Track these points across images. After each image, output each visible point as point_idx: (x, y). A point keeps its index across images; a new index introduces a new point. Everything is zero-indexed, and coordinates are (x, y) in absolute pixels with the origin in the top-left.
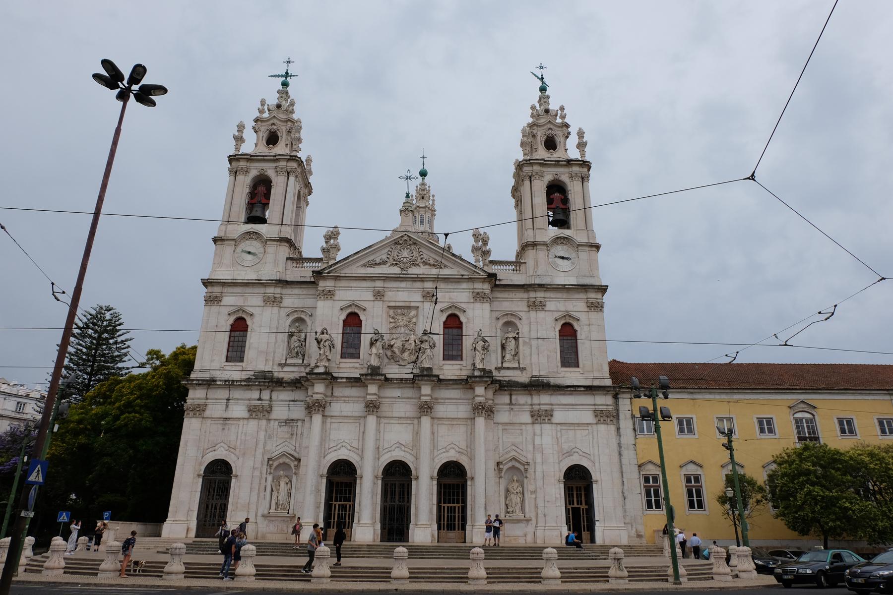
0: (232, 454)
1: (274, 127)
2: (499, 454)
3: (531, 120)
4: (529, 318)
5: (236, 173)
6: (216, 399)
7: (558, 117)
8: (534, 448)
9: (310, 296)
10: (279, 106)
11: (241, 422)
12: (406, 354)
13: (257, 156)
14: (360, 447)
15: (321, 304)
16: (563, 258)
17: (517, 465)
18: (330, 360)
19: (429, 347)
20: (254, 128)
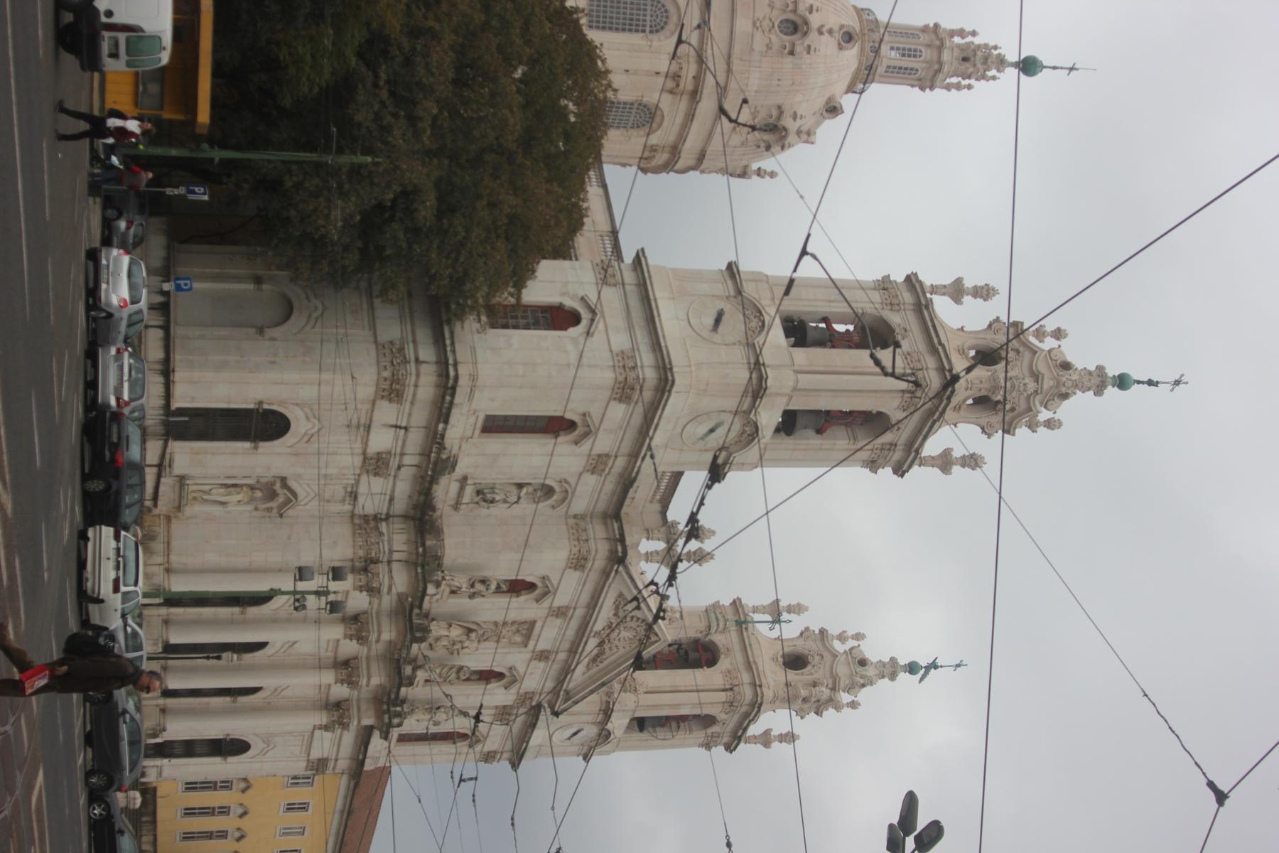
0: (295, 440)
6: (410, 415)
9: (593, 504)
16: (575, 734)
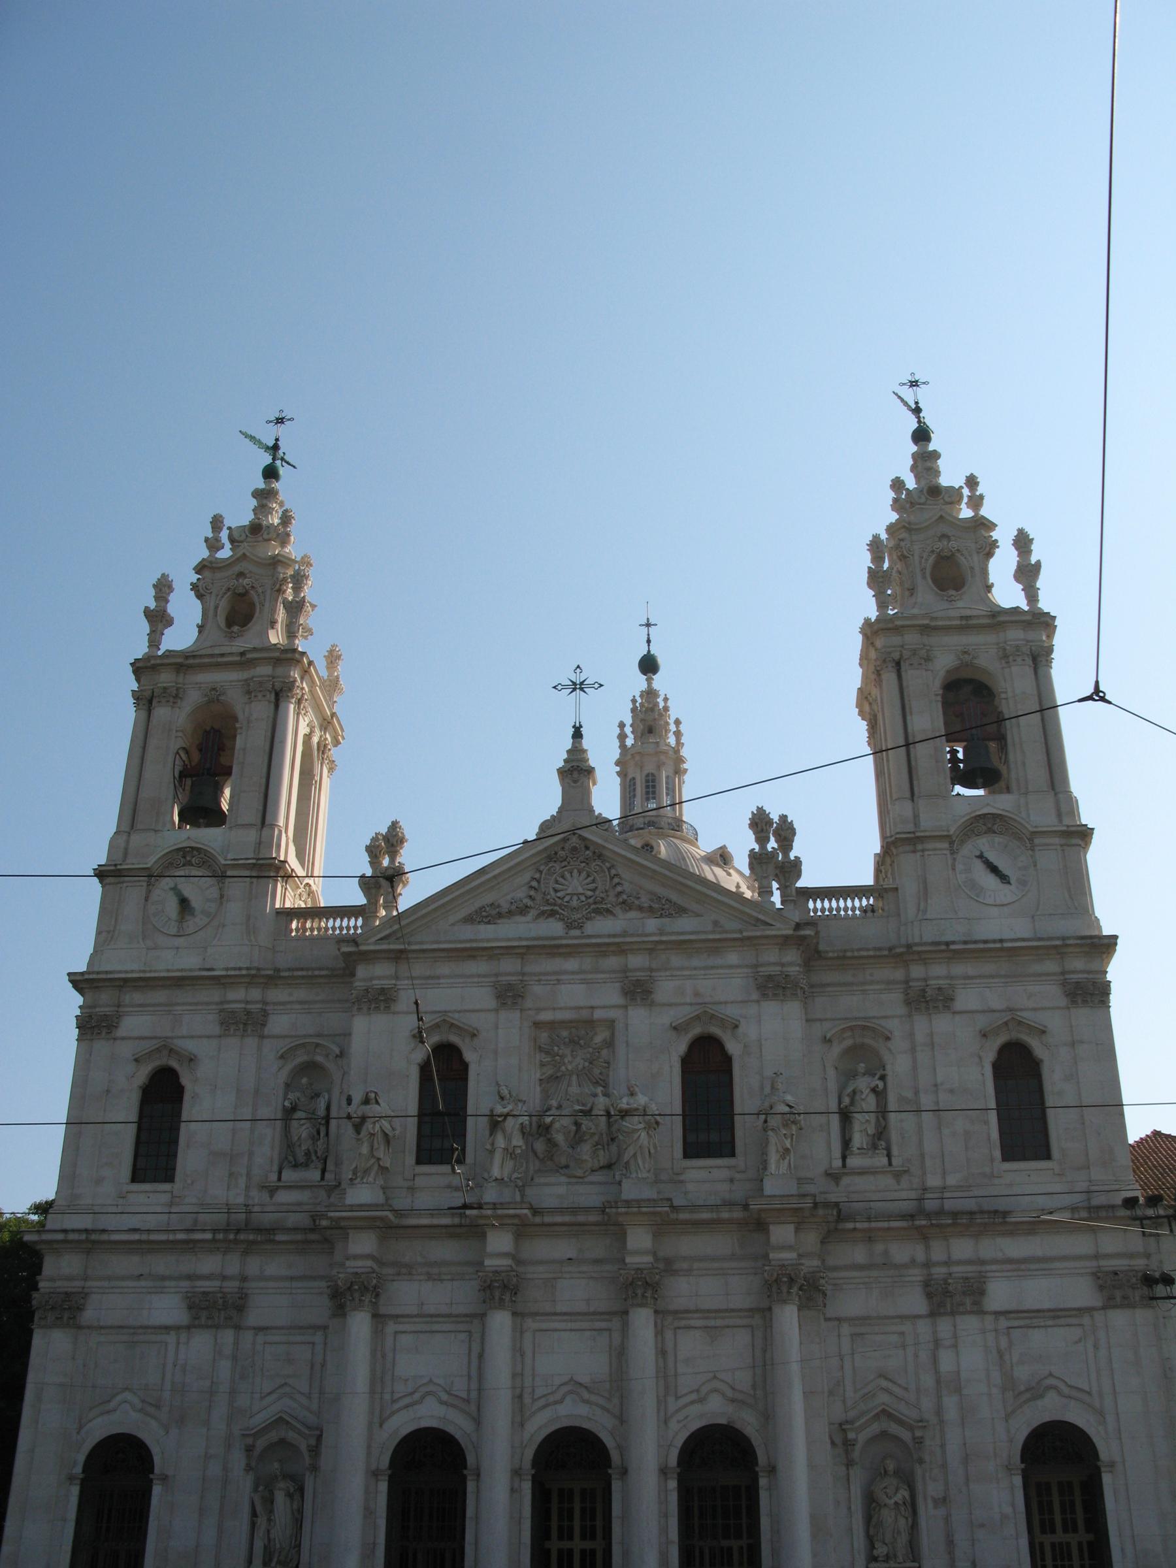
1: (246, 581)
2: (844, 1401)
3: (894, 517)
4: (911, 1035)
5: (150, 702)
7: (963, 506)
8: (938, 1382)
10: (256, 529)
11: (171, 1338)
12: (585, 1149)
13: (201, 656)
14: (474, 1395)
15: (362, 1026)
16: (994, 869)
17: (894, 1429)
18: (387, 1168)
19: (642, 1126)
20: (194, 587)
